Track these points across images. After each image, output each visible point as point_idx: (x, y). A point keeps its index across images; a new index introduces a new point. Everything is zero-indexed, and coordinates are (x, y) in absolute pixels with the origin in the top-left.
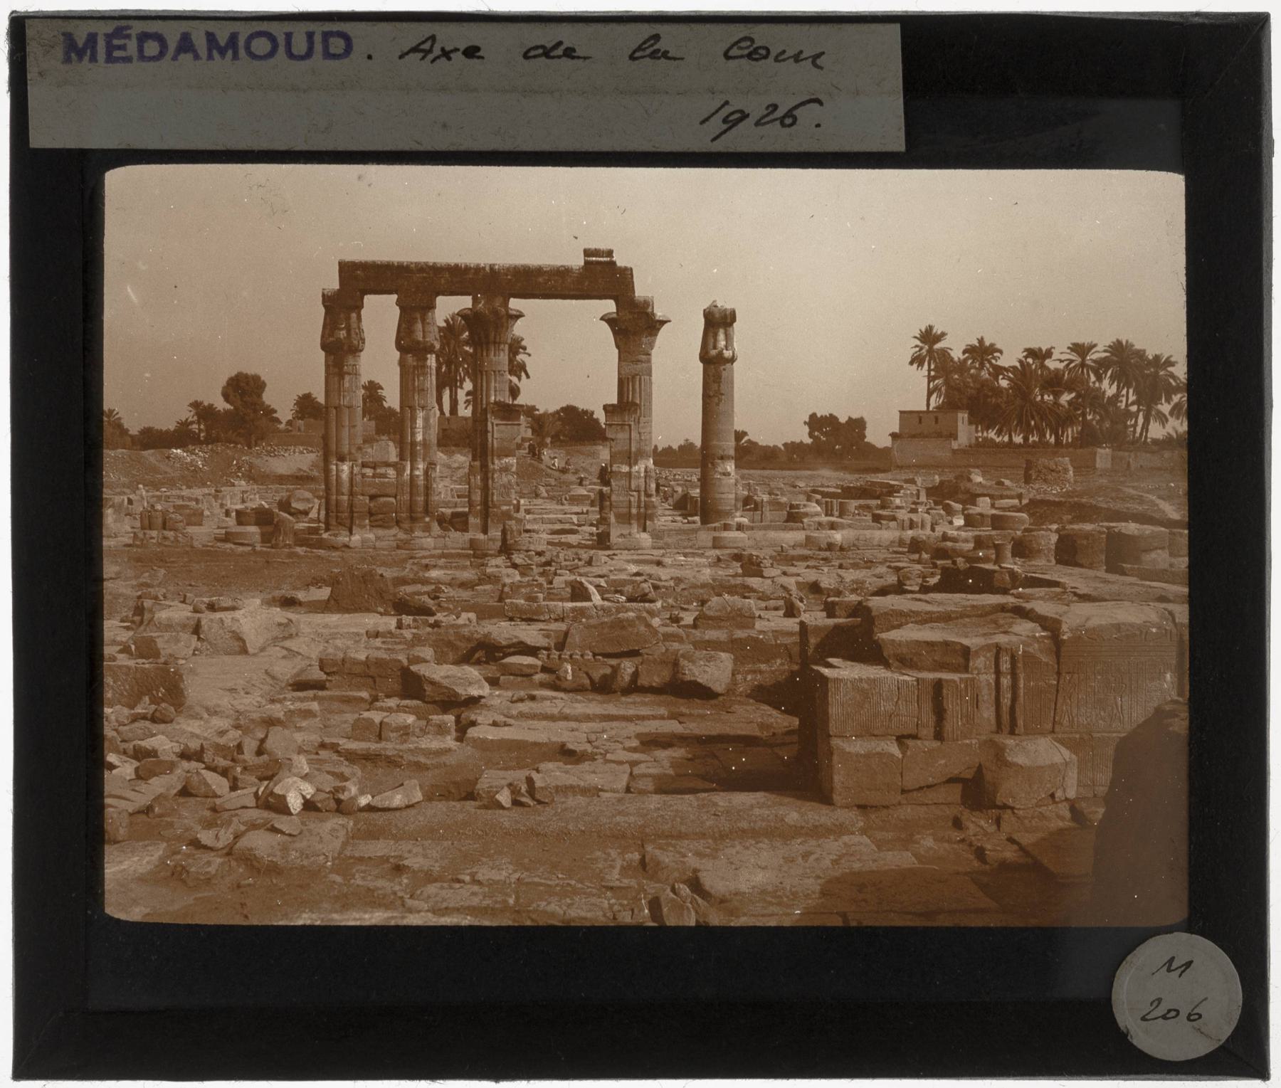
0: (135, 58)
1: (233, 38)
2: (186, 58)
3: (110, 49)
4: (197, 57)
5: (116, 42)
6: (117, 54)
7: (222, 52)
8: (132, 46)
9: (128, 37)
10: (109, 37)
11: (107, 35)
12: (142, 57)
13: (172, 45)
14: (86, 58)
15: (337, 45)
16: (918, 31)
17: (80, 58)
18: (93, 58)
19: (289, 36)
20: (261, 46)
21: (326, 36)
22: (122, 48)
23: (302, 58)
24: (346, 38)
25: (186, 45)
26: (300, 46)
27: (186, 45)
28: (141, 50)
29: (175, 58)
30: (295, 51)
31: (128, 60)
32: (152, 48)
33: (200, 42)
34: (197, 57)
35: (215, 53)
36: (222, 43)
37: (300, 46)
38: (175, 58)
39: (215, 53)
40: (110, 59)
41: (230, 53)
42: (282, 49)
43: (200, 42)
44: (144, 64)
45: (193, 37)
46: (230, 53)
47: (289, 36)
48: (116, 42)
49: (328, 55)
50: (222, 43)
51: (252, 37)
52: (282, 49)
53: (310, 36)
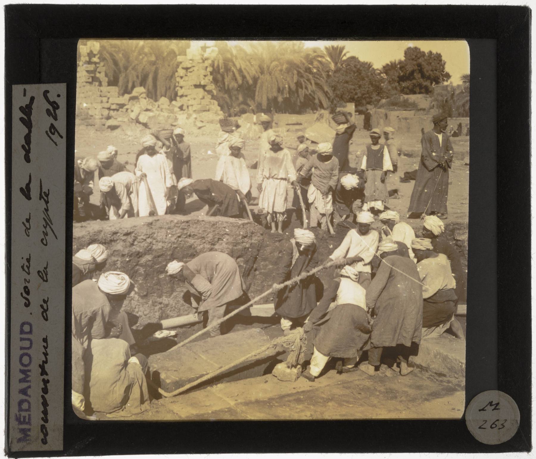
0: (28, 413)
1: (22, 371)
2: (29, 392)
3: (24, 422)
4: (29, 387)
5: (22, 420)
6: (27, 420)
7: (28, 376)
8: (23, 414)
9: (20, 415)
10: (21, 423)
11: (19, 424)
12: (28, 410)
13: (24, 397)
14: (29, 433)
15: (26, 328)
16: (12, 78)
17: (29, 436)
18: (29, 430)
19: (22, 348)
20: (26, 360)
21: (22, 332)
22: (24, 417)
23: (31, 344)
24: (23, 324)
25: (24, 392)
26: (27, 344)
27: (24, 392)
28: (26, 410)
29: (30, 396)
30: (28, 346)
31: (29, 415)
32: (25, 406)
33: (24, 385)
34: (29, 387)
35: (28, 379)
36: (24, 376)
37: (27, 344)
38: (30, 396)
39: (28, 379)
40: (29, 423)
41: (28, 373)
42: (26, 351)
43: (24, 385)
44: (32, 409)
45: (20, 388)
46: (28, 373)
47: (22, 348)
48: (22, 420)
49: (30, 332)
50: (24, 376)
51: (22, 364)
52: (26, 351)
53: (22, 339)
